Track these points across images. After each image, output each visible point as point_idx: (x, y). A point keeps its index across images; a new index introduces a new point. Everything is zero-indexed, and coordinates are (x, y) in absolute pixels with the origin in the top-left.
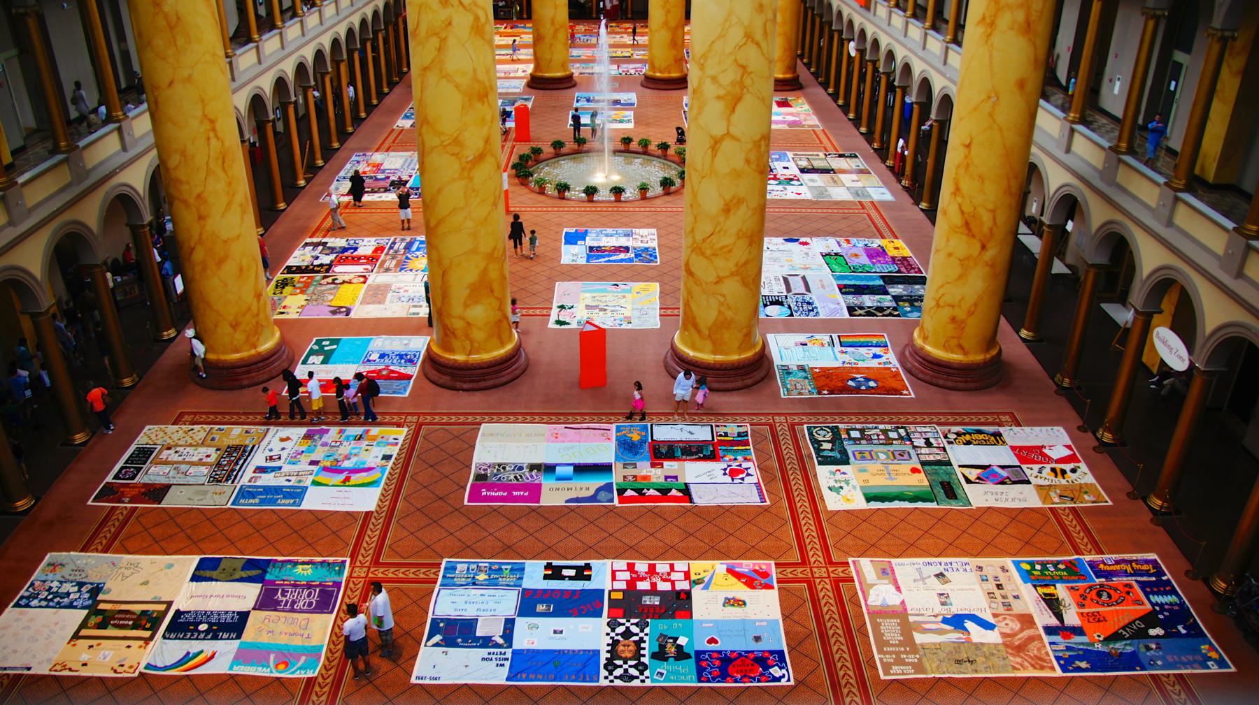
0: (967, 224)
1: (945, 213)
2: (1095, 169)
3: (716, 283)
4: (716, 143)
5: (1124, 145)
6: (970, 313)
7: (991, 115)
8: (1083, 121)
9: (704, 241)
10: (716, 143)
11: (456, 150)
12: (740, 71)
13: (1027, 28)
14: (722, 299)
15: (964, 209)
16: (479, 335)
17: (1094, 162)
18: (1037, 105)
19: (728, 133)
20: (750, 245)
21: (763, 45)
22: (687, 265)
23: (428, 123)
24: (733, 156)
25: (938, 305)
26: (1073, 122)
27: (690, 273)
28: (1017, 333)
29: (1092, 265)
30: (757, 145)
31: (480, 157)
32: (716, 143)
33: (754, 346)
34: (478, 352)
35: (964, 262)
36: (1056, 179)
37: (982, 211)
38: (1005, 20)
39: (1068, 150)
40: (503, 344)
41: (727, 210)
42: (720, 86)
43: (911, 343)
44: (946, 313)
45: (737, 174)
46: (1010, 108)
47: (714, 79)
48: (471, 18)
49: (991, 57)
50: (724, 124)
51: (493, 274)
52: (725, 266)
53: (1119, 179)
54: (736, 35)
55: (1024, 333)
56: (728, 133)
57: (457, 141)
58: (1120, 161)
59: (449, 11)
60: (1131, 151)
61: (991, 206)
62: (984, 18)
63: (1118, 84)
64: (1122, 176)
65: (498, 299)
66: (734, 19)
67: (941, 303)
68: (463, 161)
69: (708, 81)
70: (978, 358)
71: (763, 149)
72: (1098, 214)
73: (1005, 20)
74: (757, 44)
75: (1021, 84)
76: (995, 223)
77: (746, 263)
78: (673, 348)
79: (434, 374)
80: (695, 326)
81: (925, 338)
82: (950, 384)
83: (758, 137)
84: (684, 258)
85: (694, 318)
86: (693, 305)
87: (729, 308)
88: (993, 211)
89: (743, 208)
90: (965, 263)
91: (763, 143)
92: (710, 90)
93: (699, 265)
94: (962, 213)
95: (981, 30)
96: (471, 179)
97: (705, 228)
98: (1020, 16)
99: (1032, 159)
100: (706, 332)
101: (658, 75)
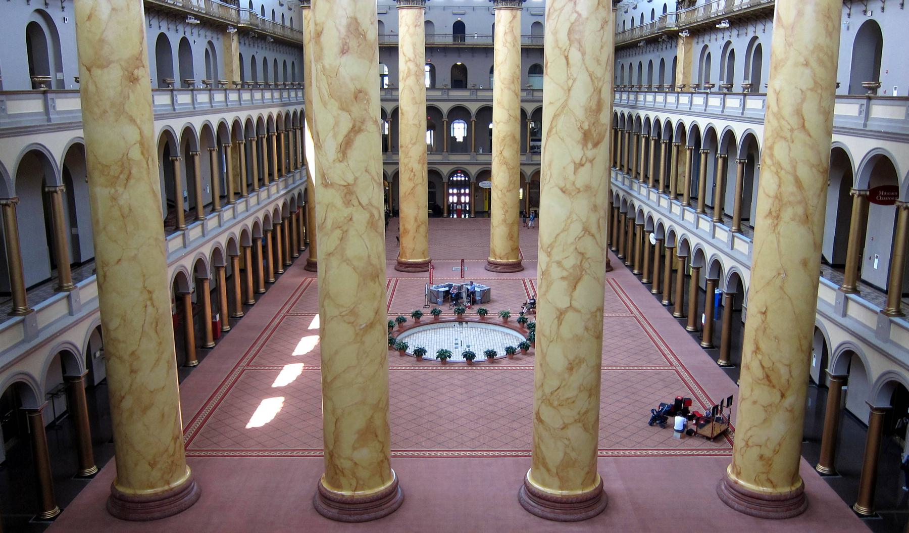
0: (767, 377)
1: (748, 368)
2: (869, 328)
3: (562, 429)
4: (561, 315)
5: (893, 310)
6: (776, 452)
7: (781, 288)
8: (855, 291)
9: (552, 393)
10: (561, 314)
11: (352, 319)
12: (580, 258)
13: (806, 219)
14: (567, 442)
15: (764, 364)
16: (363, 474)
17: (868, 324)
18: (818, 281)
19: (571, 306)
20: (590, 396)
21: (598, 236)
22: (538, 414)
23: (330, 297)
24: (574, 324)
25: (747, 445)
26: (847, 292)
27: (540, 420)
28: (815, 468)
29: (877, 409)
30: (593, 315)
31: (371, 326)
32: (561, 314)
33: (594, 481)
34: (362, 489)
35: (766, 408)
36: (836, 339)
37: (779, 365)
38: (788, 214)
39: (845, 314)
40: (383, 483)
41: (570, 369)
42: (564, 269)
43: (725, 478)
44: (754, 452)
45: (578, 339)
46: (796, 283)
47: (559, 263)
48: (368, 215)
49: (779, 242)
50: (568, 299)
51: (378, 422)
52: (569, 414)
53: (892, 337)
54: (576, 229)
55: (820, 468)
56: (571, 306)
57: (353, 312)
58: (891, 322)
59: (350, 209)
60: (899, 314)
61: (787, 362)
62: (770, 212)
63: (876, 261)
64: (895, 334)
65: (380, 442)
66: (574, 217)
67: (750, 443)
68: (357, 328)
69: (554, 265)
70: (785, 490)
71: (598, 316)
72: (876, 367)
73: (788, 214)
74: (593, 235)
75: (805, 263)
76: (791, 376)
77: (586, 412)
78: (526, 483)
79: (323, 507)
80: (545, 465)
81: (738, 474)
82: (763, 513)
83: (594, 309)
84: (535, 408)
85: (544, 459)
86: (543, 447)
87: (573, 449)
88: (789, 366)
89: (584, 366)
90: (768, 408)
91: (598, 314)
92: (556, 272)
93: (547, 414)
94: (763, 367)
95: (769, 221)
96: (363, 343)
97: (554, 383)
98: (800, 210)
99: (817, 324)
100: (554, 470)
101: (499, 260)
